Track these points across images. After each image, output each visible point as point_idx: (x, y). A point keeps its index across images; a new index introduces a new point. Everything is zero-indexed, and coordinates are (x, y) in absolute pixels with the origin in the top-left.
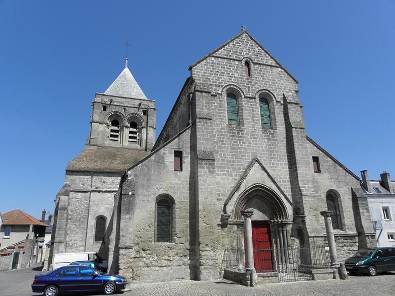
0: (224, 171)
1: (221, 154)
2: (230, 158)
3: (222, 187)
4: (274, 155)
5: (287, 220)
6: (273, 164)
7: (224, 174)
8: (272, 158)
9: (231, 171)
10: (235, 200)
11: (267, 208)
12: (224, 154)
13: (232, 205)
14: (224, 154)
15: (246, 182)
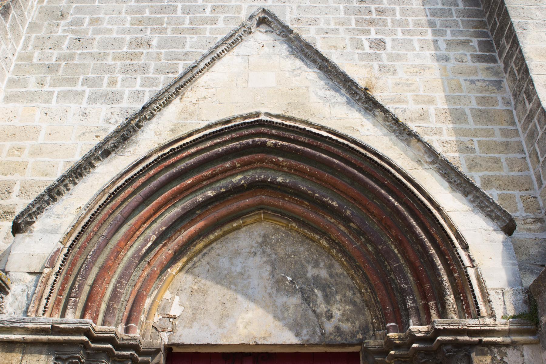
0: (72, 81)
1: (79, 22)
2: (123, 31)
3: (37, 152)
4: (379, 12)
5: (472, 323)
6: (379, 44)
7: (65, 95)
8: (371, 23)
9: (113, 82)
10: (83, 203)
11: (338, 269)
12: (94, 21)
13: (54, 231)
14: (95, 21)
15: (183, 111)
